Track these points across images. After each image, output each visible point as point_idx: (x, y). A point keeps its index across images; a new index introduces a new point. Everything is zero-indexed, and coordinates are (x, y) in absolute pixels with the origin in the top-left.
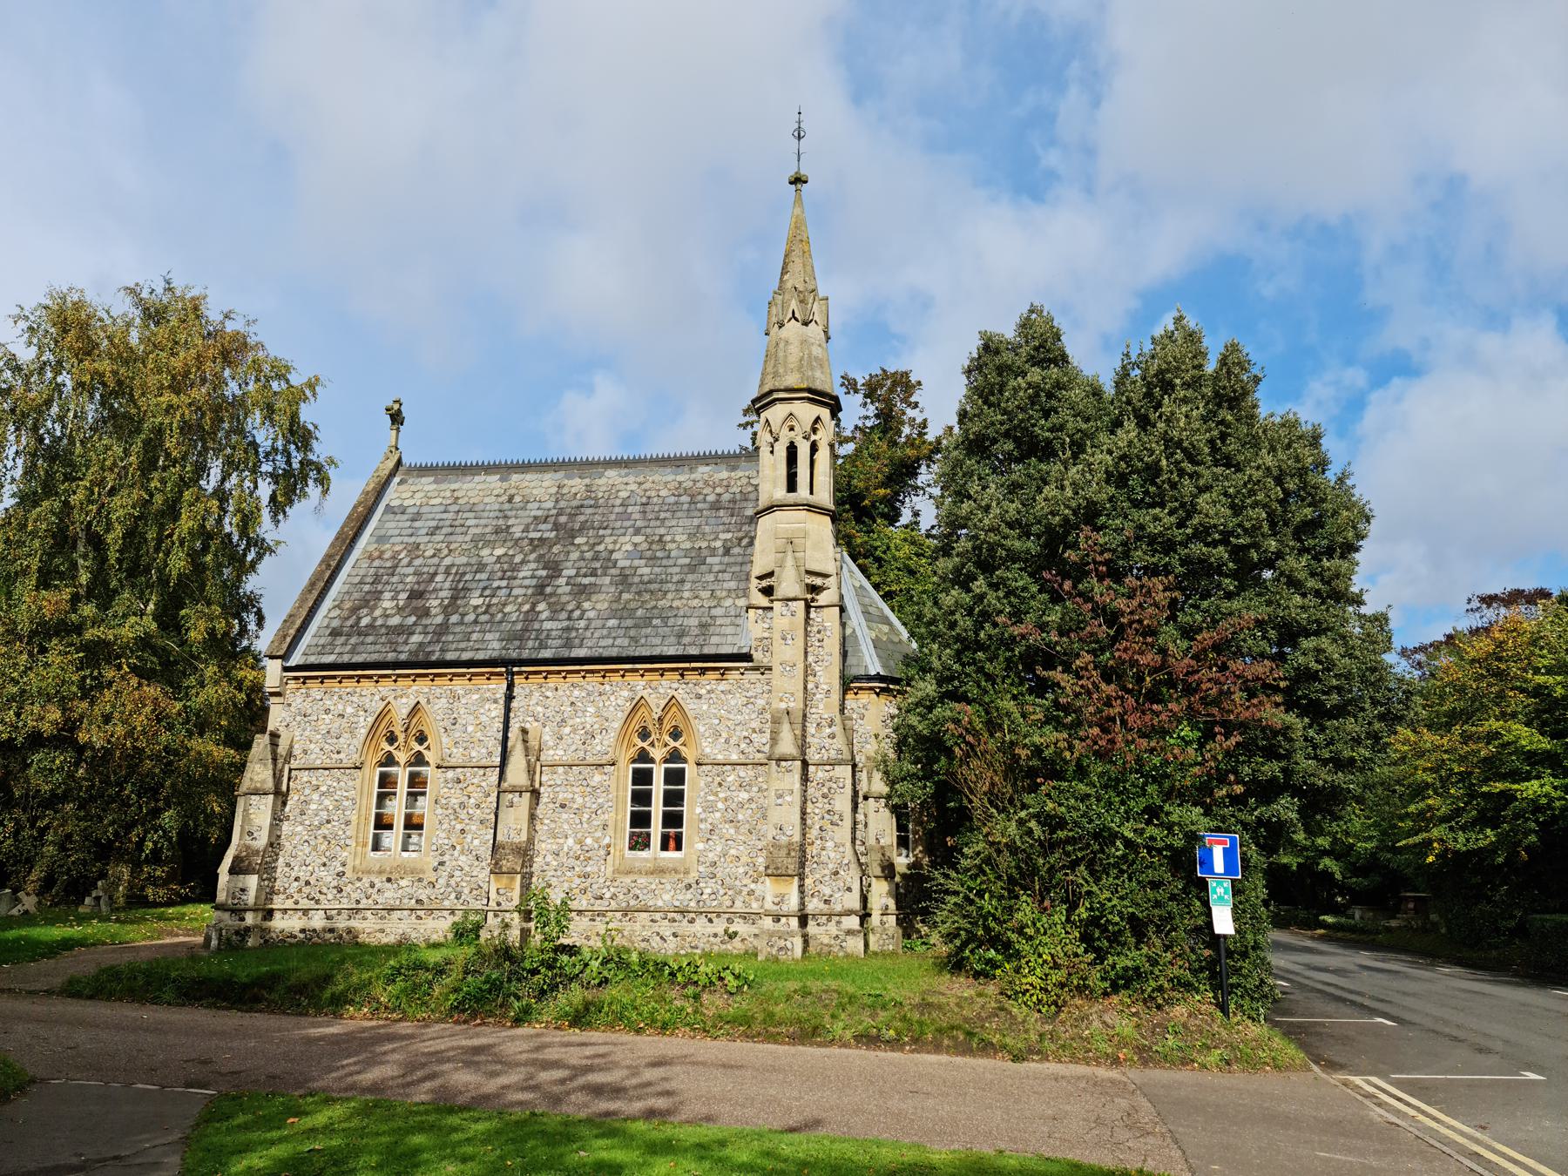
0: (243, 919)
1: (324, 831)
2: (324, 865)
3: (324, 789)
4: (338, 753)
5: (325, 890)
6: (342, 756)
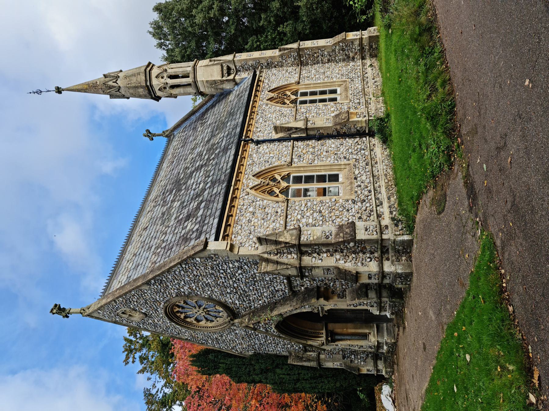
0: (387, 227)
1: (326, 213)
2: (348, 210)
3: (299, 217)
4: (277, 212)
5: (364, 208)
6: (279, 210)
